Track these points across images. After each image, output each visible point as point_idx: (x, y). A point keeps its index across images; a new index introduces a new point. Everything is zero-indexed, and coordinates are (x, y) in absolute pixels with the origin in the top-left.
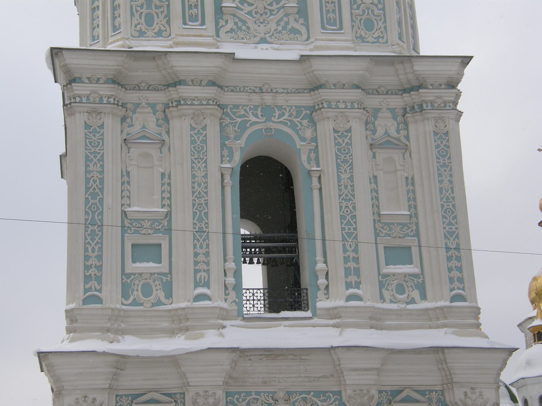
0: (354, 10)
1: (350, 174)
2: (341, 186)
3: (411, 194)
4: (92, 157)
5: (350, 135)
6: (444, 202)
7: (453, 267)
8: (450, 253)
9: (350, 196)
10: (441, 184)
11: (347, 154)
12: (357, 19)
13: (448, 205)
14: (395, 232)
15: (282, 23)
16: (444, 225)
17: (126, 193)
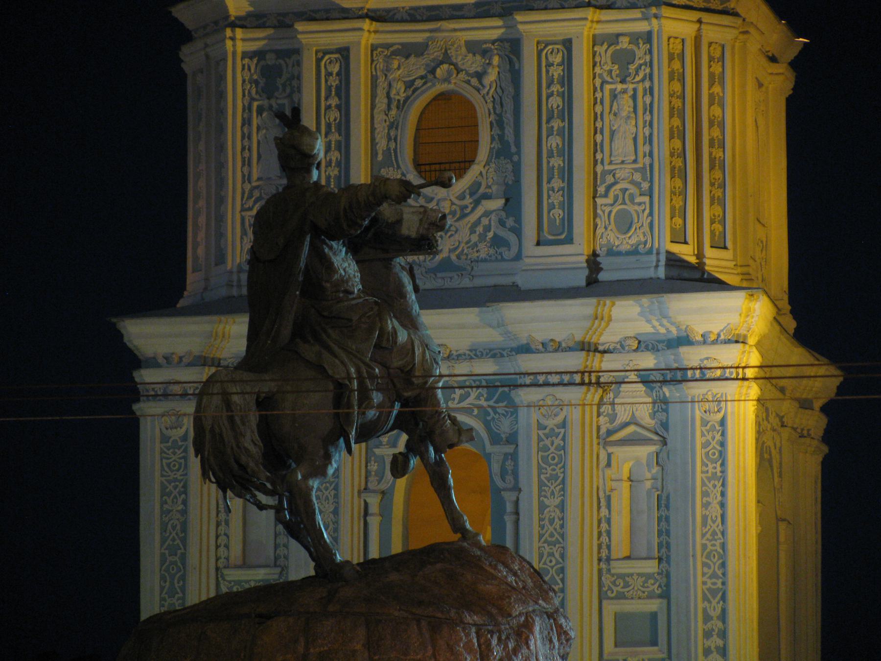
0: (601, 196)
1: (560, 499)
2: (543, 520)
3: (663, 524)
4: (170, 487)
5: (563, 430)
6: (708, 539)
7: (713, 649)
8: (709, 625)
9: (556, 535)
10: (706, 509)
11: (556, 465)
12: (604, 212)
13: (713, 545)
14: (633, 588)
15: (480, 229)
16: (705, 579)
17: (222, 540)
